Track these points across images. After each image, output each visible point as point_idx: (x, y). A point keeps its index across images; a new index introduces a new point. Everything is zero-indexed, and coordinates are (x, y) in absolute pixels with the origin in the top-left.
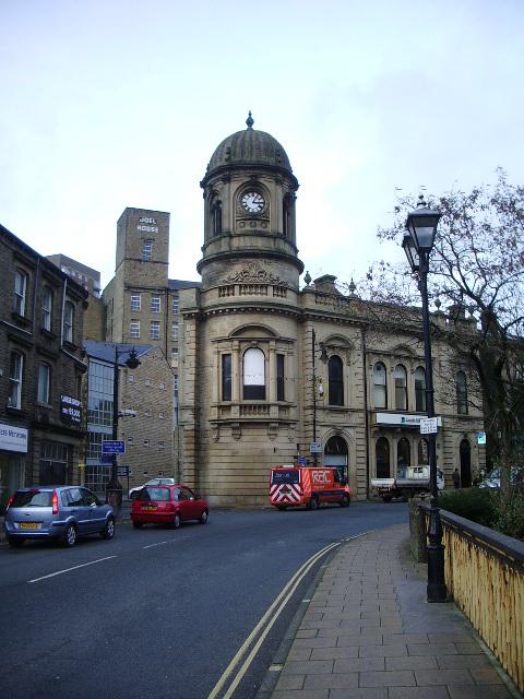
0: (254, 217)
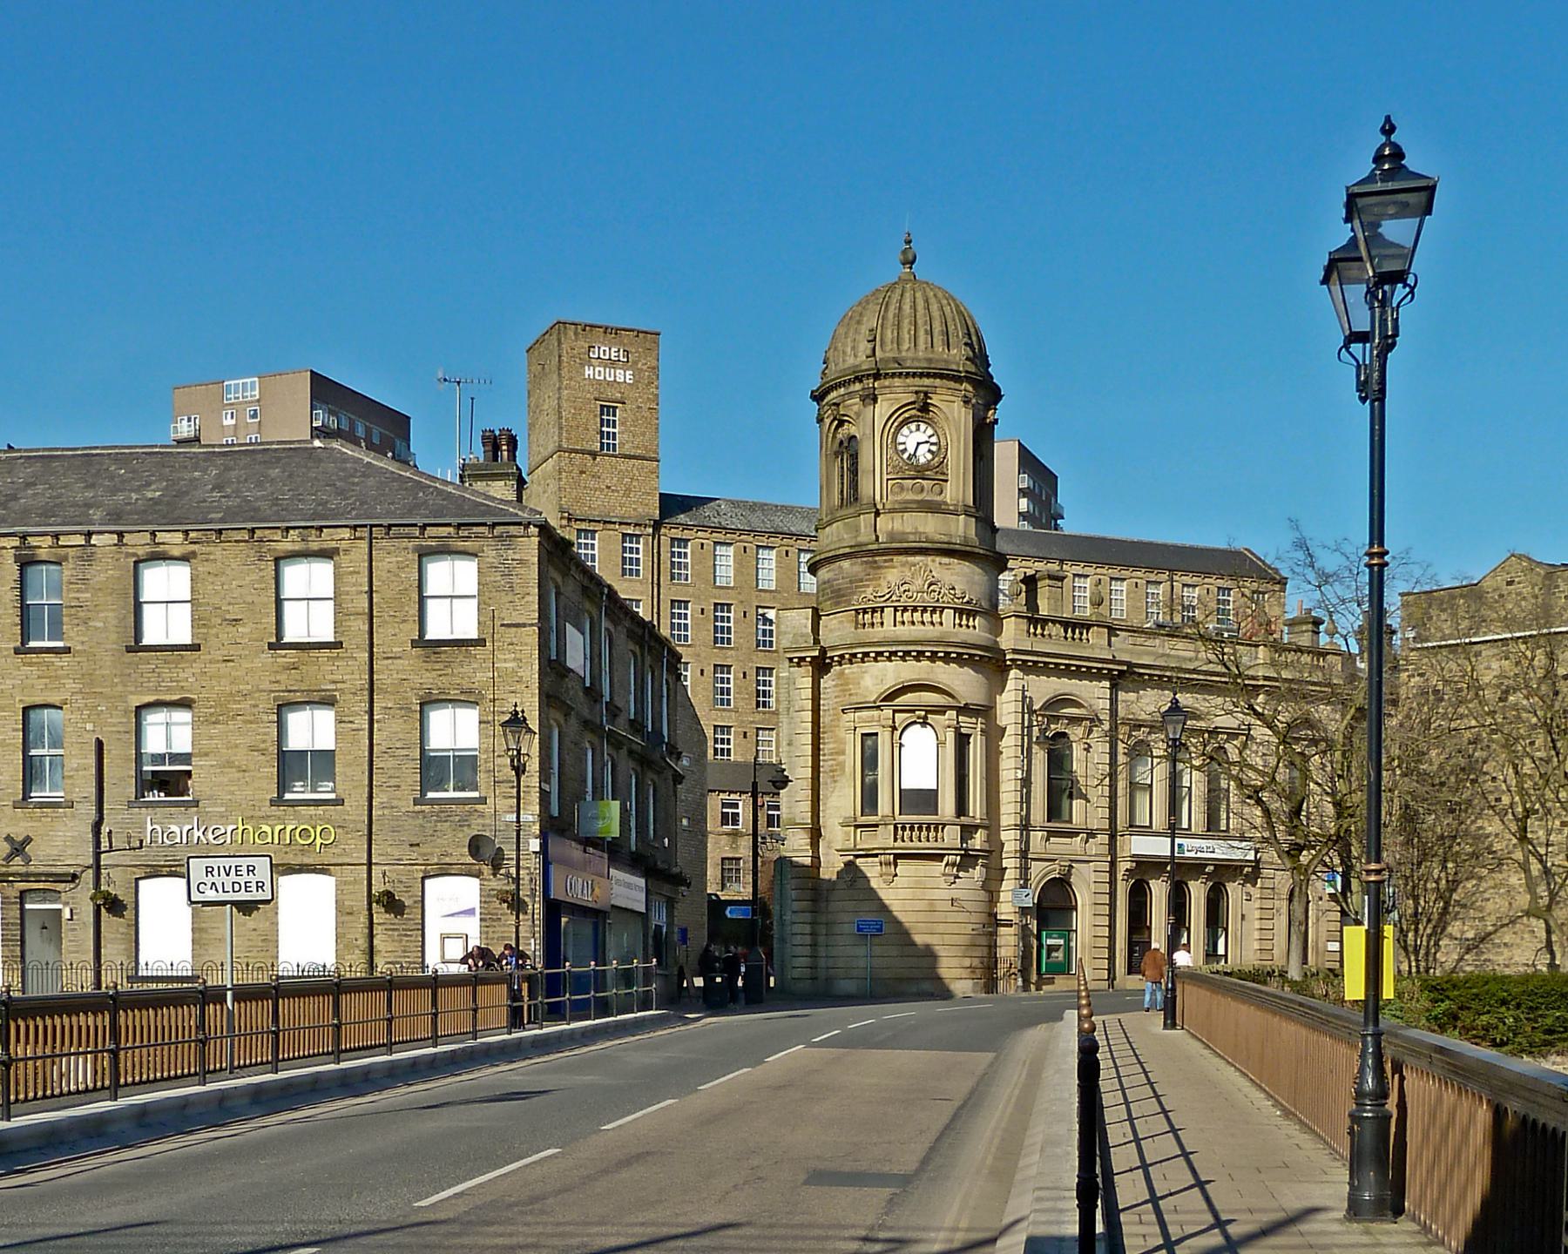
0: (920, 472)
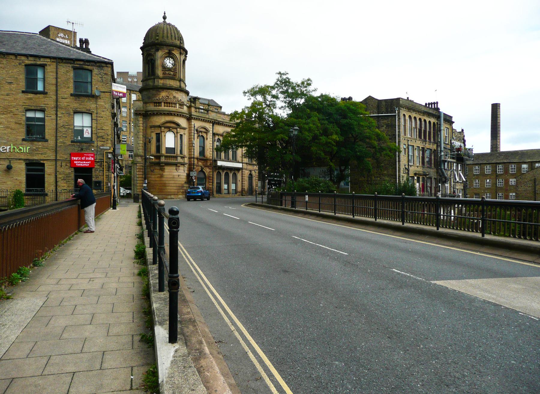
0: (170, 69)
